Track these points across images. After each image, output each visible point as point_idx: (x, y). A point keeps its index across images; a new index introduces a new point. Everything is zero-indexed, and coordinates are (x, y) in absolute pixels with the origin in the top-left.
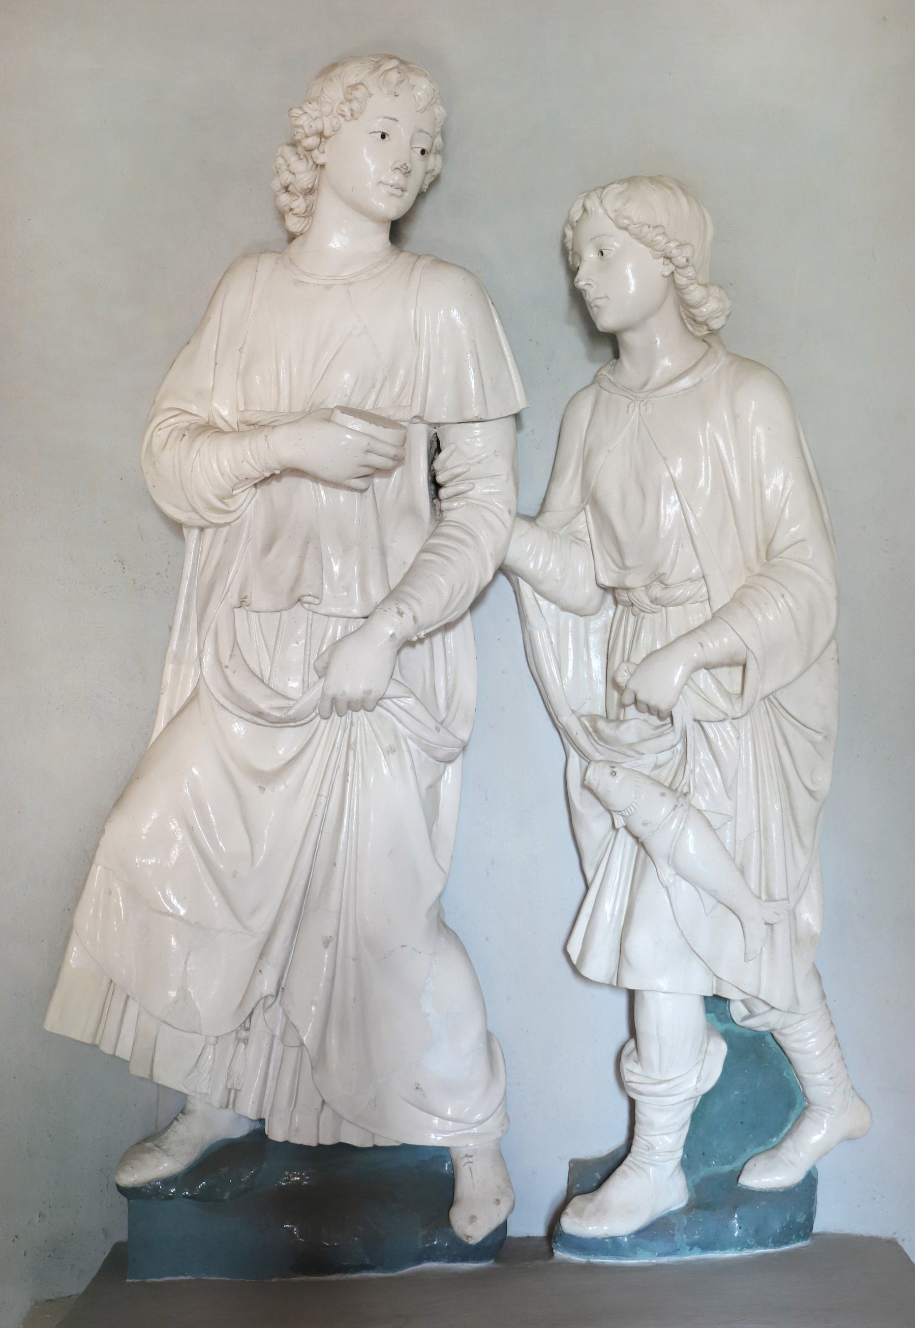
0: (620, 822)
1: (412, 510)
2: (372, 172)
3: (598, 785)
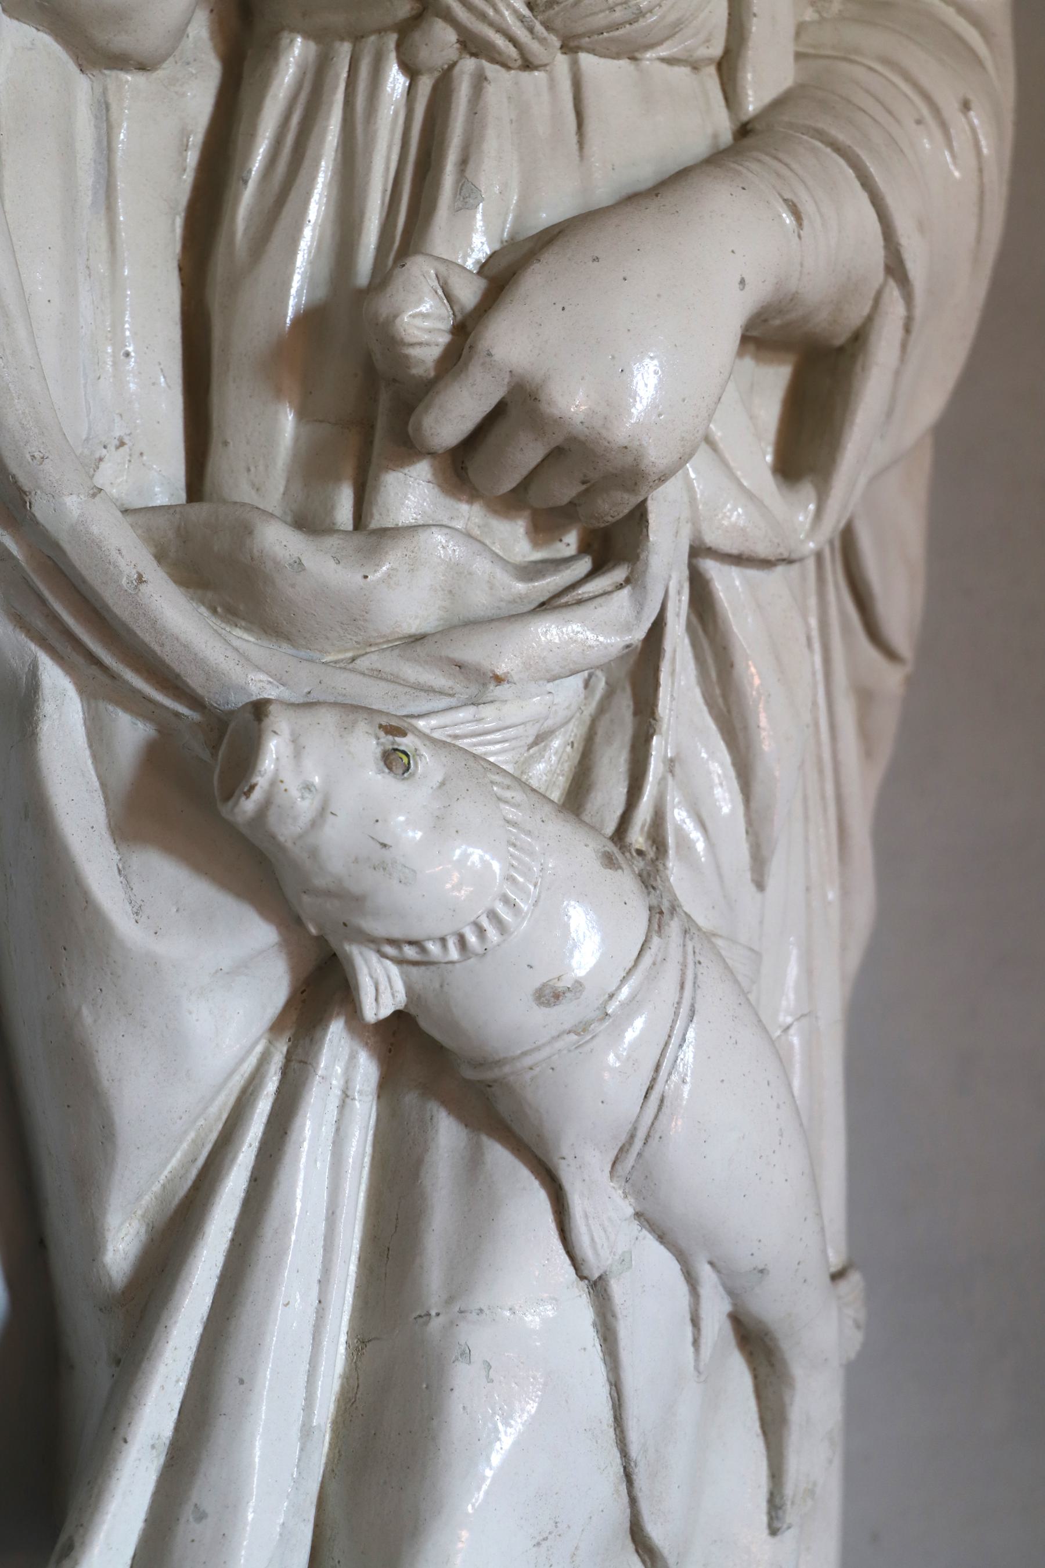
0: (381, 988)
3: (323, 812)
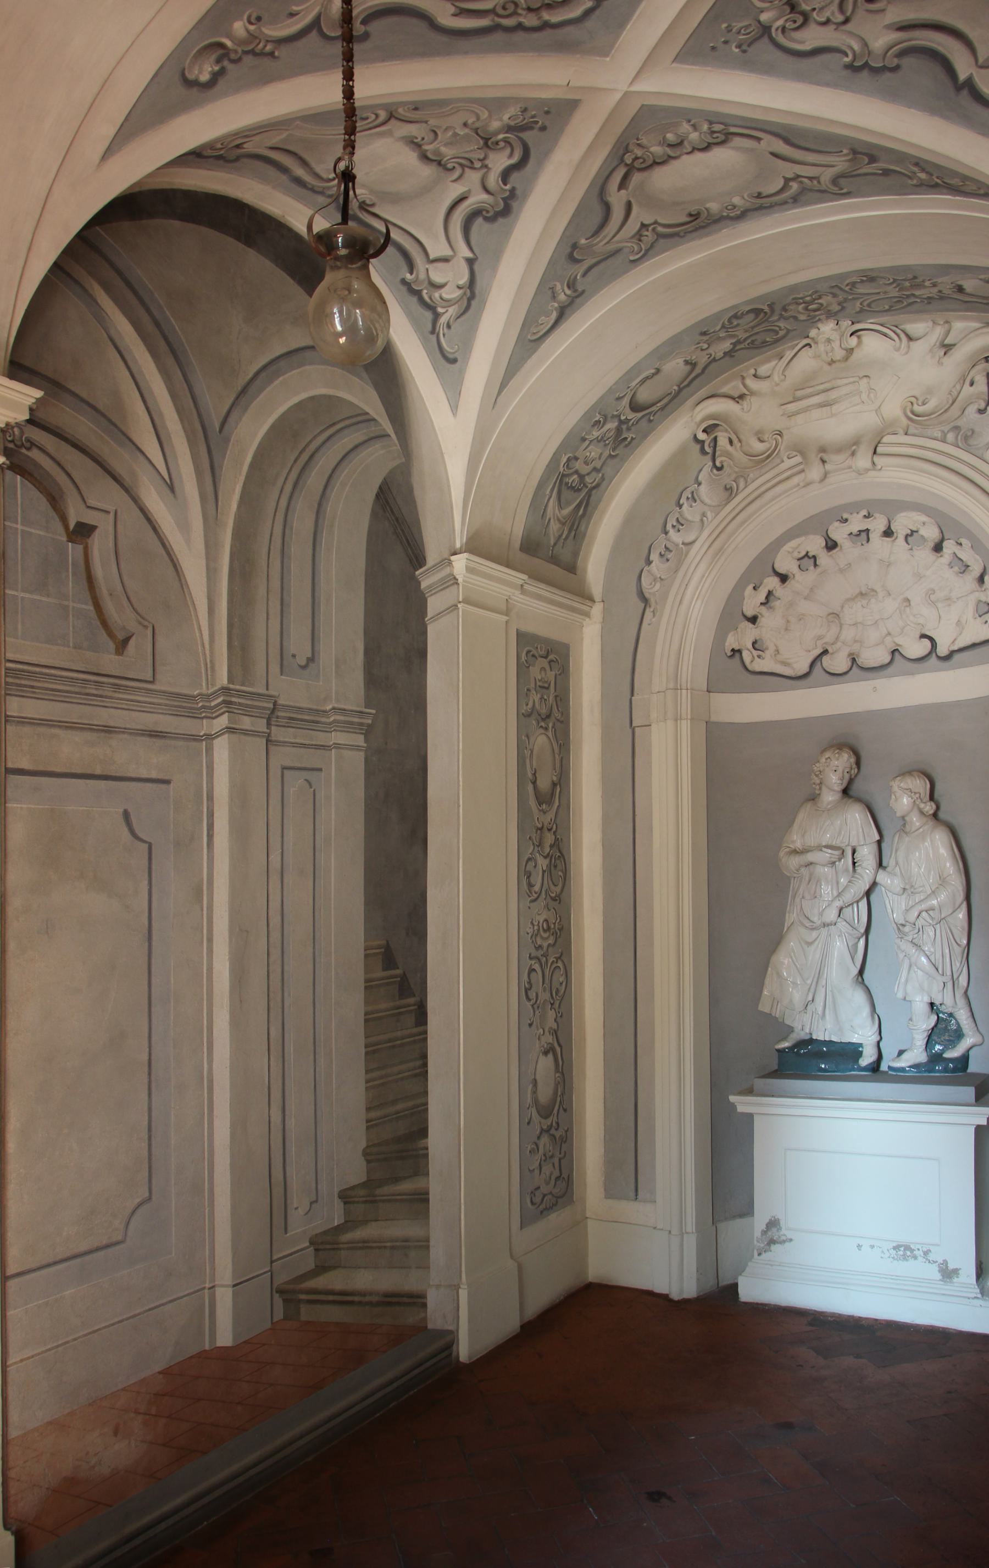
1: (847, 870)
2: (835, 781)
